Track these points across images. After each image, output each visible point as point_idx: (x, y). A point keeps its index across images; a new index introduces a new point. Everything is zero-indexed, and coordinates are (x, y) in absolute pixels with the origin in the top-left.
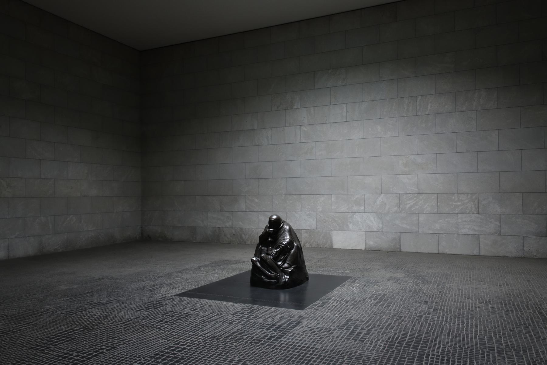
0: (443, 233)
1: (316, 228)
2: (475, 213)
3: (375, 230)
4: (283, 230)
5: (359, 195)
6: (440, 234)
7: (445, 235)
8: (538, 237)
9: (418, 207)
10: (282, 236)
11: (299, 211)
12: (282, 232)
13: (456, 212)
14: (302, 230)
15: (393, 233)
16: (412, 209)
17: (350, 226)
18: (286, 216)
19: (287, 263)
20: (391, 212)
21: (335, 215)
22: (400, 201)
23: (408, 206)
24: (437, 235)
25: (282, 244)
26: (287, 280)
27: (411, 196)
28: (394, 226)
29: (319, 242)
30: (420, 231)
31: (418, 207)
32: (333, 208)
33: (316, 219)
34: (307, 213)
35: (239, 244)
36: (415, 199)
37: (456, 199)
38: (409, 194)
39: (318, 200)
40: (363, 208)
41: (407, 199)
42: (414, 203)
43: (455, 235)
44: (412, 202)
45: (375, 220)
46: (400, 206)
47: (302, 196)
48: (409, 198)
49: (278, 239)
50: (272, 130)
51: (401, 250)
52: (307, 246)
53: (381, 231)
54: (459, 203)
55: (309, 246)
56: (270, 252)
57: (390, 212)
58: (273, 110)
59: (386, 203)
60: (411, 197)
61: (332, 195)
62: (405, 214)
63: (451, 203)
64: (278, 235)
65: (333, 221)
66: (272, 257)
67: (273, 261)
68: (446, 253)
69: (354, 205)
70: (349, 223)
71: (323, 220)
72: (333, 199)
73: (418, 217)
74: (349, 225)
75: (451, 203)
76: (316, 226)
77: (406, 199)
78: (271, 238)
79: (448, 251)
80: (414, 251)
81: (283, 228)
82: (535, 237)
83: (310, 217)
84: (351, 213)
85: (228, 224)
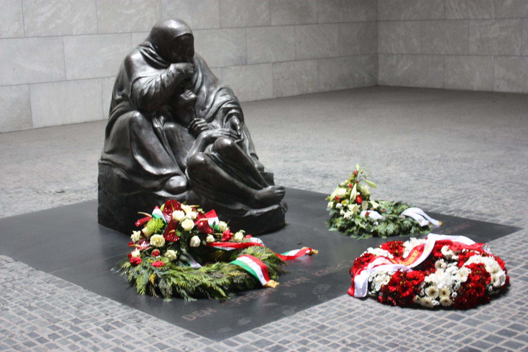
0: (109, 75)
6: (104, 78)
8: (238, 67)
9: (60, 21)
12: (199, 69)
15: (14, 87)
22: (24, 9)
24: (98, 82)
28: (14, 69)
30: (69, 77)
31: (60, 21)
51: (32, 125)
54: (133, 11)
57: (3, 36)
62: (36, 39)
64: (194, 81)
73: (63, 44)
77: (36, 2)
80: (60, 123)
82: (234, 68)
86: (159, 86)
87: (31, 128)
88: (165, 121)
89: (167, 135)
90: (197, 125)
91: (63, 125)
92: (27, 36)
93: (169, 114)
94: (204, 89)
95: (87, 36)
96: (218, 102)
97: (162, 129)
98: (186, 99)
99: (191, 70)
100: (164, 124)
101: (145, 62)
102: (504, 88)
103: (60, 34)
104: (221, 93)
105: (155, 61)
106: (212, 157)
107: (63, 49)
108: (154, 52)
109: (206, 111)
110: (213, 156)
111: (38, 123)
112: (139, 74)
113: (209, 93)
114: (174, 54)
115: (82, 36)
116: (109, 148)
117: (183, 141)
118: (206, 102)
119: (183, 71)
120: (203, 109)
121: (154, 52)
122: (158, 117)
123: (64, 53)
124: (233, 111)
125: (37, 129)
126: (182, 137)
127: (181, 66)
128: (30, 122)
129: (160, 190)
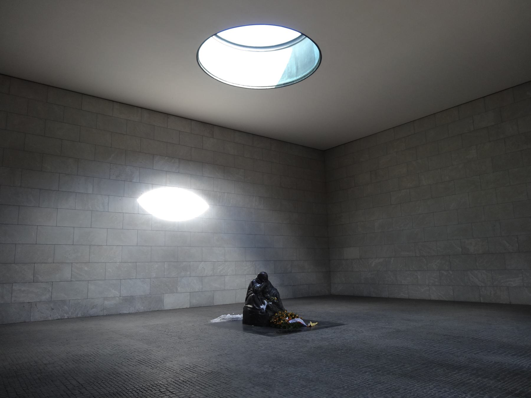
1: (150, 293)
2: (254, 274)
3: (197, 290)
11: (134, 278)
17: (179, 289)
23: (219, 270)
31: (224, 271)
32: (165, 274)
35: (59, 319)
40: (189, 273)
47: (138, 264)
50: (109, 197)
54: (246, 268)
58: (111, 178)
65: (165, 286)
69: (182, 271)
70: (178, 286)
74: (178, 288)
85: (43, 298)
96: (274, 292)
102: (374, 295)
104: (274, 290)
107: (225, 280)
112: (255, 285)
114: (263, 280)
116: (246, 303)
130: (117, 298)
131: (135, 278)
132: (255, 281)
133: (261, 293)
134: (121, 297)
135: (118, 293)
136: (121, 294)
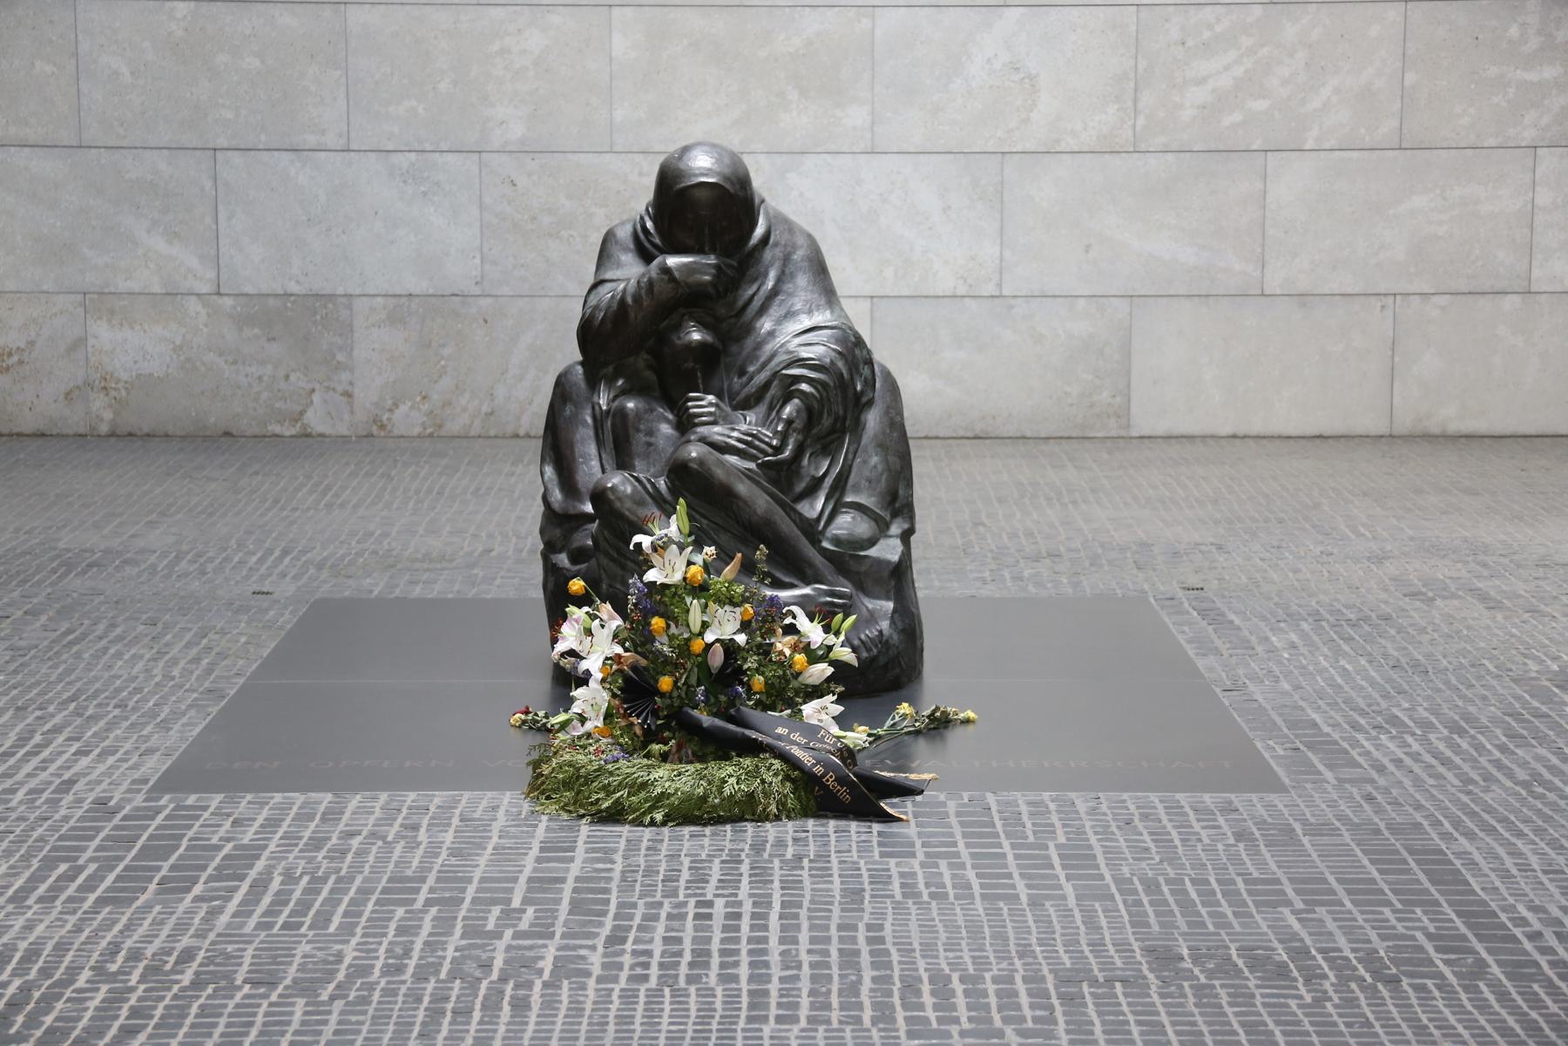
3: (945, 282)
4: (777, 264)
5: (830, 12)
7: (1442, 300)
9: (1260, 105)
10: (775, 311)
11: (331, 140)
13: (1526, 134)
14: (359, 304)
15: (1082, 302)
16: (1227, 121)
18: (208, 185)
19: (858, 507)
20: (1070, 143)
21: (641, 174)
22: (1142, 64)
23: (1199, 95)
25: (800, 362)
26: (885, 625)
27: (1218, 20)
28: (1088, 248)
29: (501, 391)
31: (1260, 105)
32: (619, 115)
33: (481, 207)
34: (396, 159)
36: (1246, 41)
37: (1534, 43)
38: (1208, 9)
39: (496, 47)
41: (1190, 43)
42: (1239, 71)
43: (1511, 302)
44: (1226, 68)
45: (946, 209)
46: (1135, 101)
48: (1207, 34)
49: (749, 329)
51: (1128, 426)
52: (396, 432)
53: (990, 289)
55: (416, 431)
56: (717, 429)
59: (1032, 78)
60: (1218, 29)
61: (616, 11)
62: (1170, 156)
63: (1494, 71)
64: (740, 303)
66: (752, 466)
67: (771, 495)
68: (1436, 430)
71: (534, 219)
72: (619, 45)
75: (1494, 71)
76: (478, 261)
78: (703, 325)
79: (1450, 417)
80: (1226, 430)
81: (776, 245)
83: (425, 194)
84: (762, 157)
86: (615, 306)
87: (1123, 433)
88: (625, 392)
89: (613, 425)
90: (688, 408)
91: (1234, 436)
92: (1143, 147)
93: (650, 376)
94: (766, 325)
95: (1355, 154)
97: (604, 408)
98: (679, 342)
99: (707, 274)
100: (616, 397)
101: (632, 246)
103: (1254, 147)
105: (647, 244)
106: (649, 486)
108: (649, 225)
109: (744, 379)
110: (653, 484)
111: (1145, 422)
113: (771, 334)
115: (1338, 153)
117: (649, 444)
118: (752, 357)
119: (676, 274)
120: (742, 372)
121: (649, 225)
122: (610, 382)
123: (1264, 207)
124: (804, 387)
125: (1142, 437)
126: (650, 433)
127: (673, 261)
128: (1123, 413)
129: (560, 552)
130: (193, 305)
131: (341, 144)
132: (624, 233)
133: (641, 361)
134: (228, 302)
135: (194, 262)
136: (223, 277)
